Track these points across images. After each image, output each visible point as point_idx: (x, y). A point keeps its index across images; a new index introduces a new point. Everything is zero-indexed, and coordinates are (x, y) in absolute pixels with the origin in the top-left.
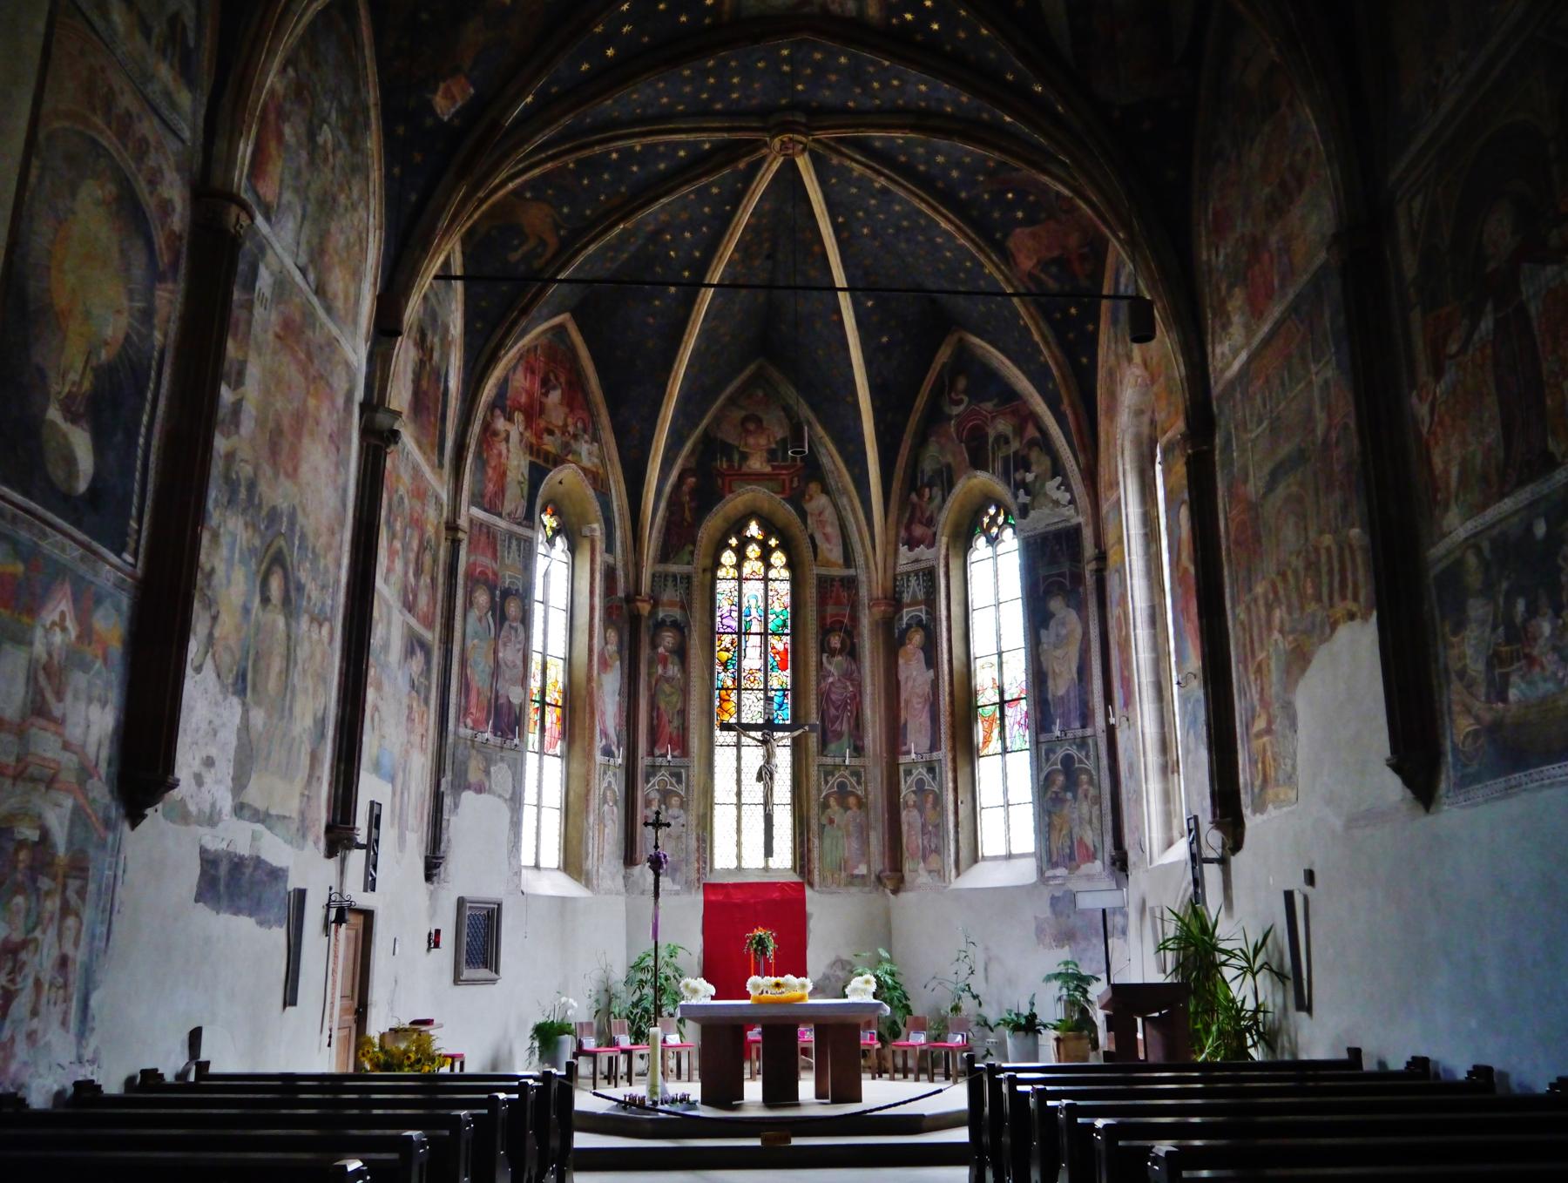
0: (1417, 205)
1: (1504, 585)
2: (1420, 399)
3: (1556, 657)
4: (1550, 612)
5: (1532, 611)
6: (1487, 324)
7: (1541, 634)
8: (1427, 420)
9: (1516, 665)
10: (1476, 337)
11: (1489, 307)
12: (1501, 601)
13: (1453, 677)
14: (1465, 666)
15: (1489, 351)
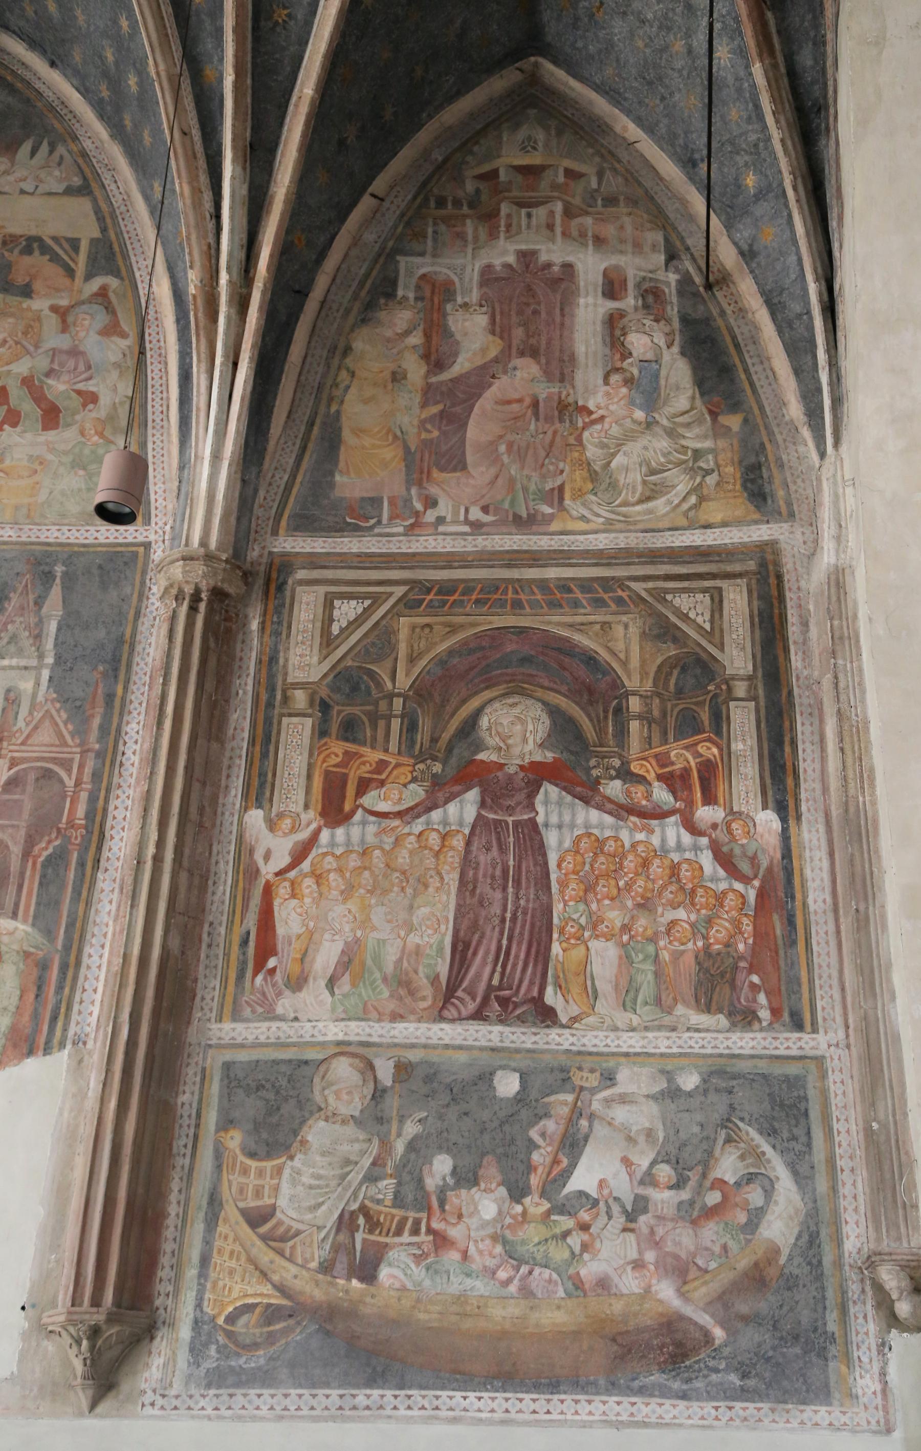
0: (346, 611)
1: (411, 1129)
2: (272, 825)
3: (499, 1249)
4: (503, 1191)
5: (466, 1178)
6: (465, 808)
7: (476, 1211)
8: (282, 860)
9: (406, 1238)
10: (436, 815)
11: (473, 795)
12: (400, 1147)
13: (231, 1212)
14: (274, 1208)
15: (458, 843)
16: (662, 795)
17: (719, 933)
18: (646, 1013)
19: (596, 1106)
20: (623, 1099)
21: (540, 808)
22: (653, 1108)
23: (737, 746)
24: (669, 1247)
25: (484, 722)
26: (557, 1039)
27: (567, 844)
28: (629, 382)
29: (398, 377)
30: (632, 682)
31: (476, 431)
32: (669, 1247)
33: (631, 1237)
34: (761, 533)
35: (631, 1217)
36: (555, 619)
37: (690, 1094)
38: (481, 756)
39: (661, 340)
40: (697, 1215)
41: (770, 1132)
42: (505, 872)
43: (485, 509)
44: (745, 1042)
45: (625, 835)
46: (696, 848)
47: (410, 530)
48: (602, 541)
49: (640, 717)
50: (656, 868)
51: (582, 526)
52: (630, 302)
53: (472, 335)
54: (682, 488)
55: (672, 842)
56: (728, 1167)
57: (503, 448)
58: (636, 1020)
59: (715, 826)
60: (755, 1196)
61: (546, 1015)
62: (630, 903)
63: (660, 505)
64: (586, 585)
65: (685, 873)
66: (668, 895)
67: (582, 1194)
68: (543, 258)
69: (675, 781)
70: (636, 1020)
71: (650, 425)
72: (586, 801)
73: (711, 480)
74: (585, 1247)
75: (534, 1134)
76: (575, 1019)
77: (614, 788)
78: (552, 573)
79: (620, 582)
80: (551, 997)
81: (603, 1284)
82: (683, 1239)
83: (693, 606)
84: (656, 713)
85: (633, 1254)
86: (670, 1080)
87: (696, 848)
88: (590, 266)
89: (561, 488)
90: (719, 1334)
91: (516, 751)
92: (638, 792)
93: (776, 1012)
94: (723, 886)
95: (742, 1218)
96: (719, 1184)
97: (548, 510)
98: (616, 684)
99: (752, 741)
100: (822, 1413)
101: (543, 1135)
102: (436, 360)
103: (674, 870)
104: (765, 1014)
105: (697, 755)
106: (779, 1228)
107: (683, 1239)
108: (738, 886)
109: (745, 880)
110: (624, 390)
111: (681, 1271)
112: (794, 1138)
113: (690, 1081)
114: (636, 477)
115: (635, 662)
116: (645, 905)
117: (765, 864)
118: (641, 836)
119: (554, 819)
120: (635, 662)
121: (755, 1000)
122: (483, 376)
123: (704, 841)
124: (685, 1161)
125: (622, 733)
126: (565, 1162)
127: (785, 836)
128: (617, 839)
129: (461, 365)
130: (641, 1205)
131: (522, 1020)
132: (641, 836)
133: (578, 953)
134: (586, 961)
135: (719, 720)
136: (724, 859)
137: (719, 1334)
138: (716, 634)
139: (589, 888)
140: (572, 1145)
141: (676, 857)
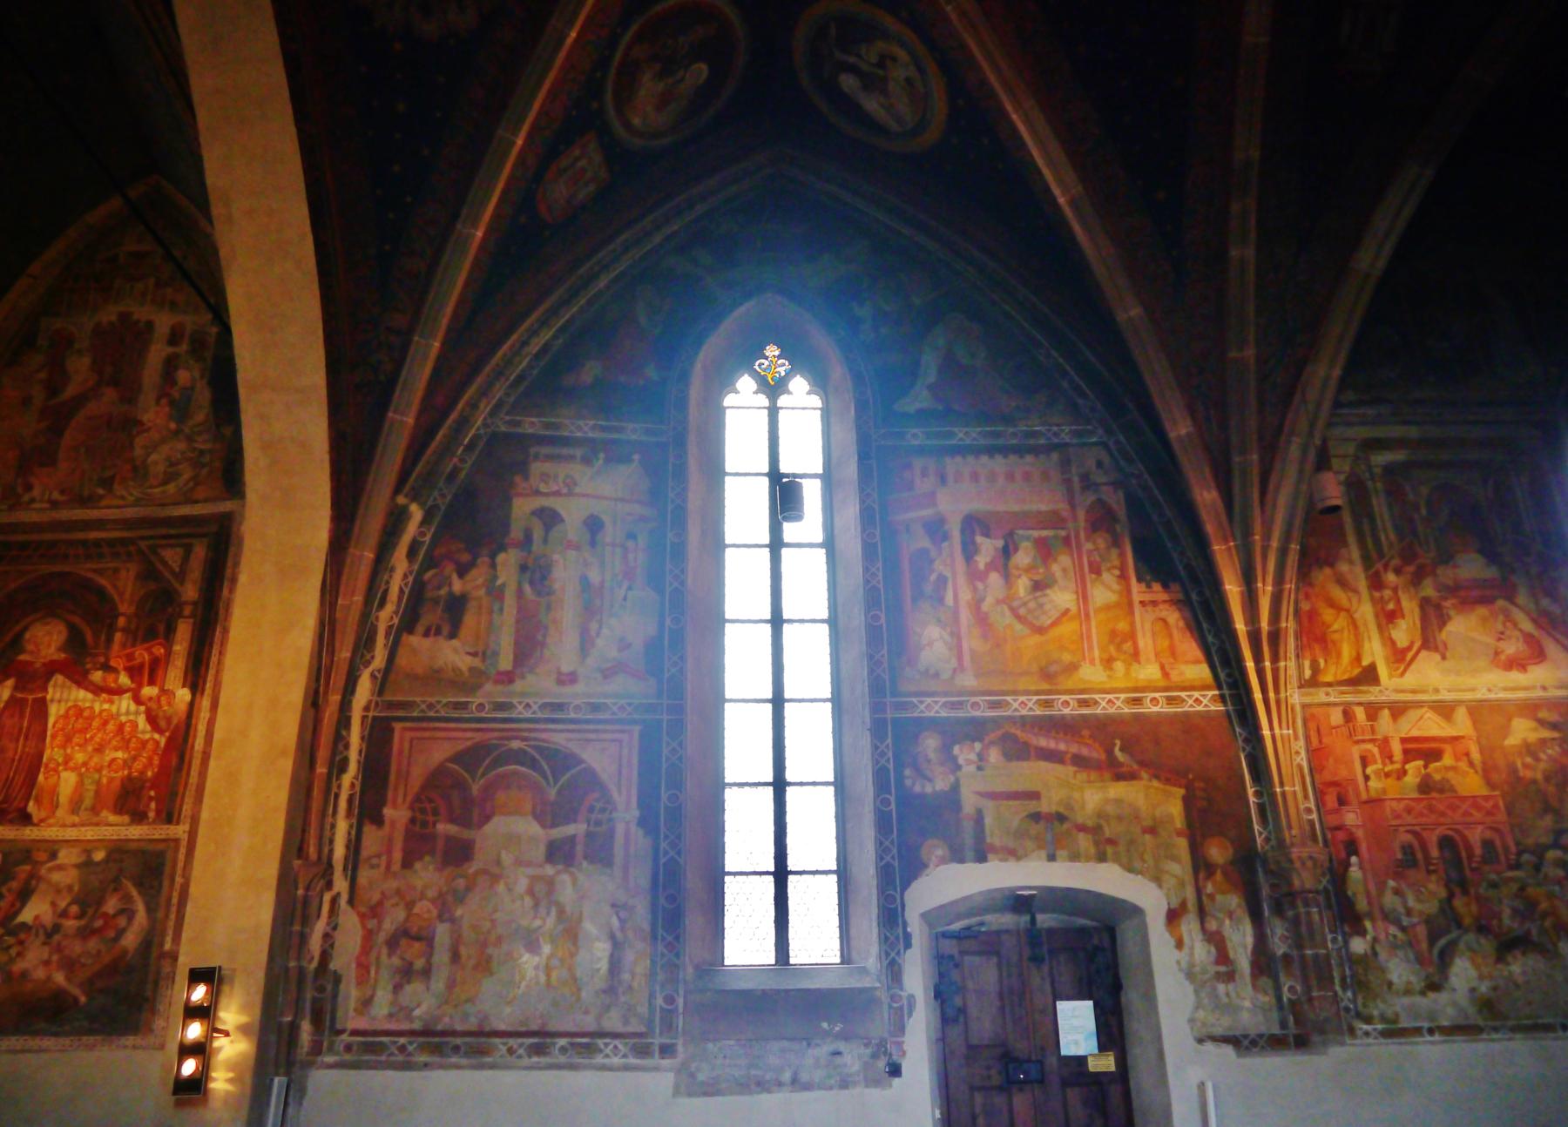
11: (10, 683)
16: (124, 680)
17: (138, 766)
18: (84, 815)
19: (43, 871)
20: (60, 868)
21: (50, 690)
22: (74, 873)
23: (177, 648)
24: (67, 952)
25: (27, 635)
26: (29, 833)
27: (62, 712)
28: (172, 403)
29: (26, 401)
30: (123, 608)
31: (68, 438)
32: (67, 952)
33: (46, 949)
34: (226, 506)
35: (49, 935)
36: (88, 566)
37: (98, 864)
38: (22, 657)
39: (197, 374)
40: (85, 933)
41: (139, 885)
42: (21, 729)
43: (62, 492)
44: (136, 832)
45: (97, 708)
46: (137, 713)
47: (11, 508)
48: (130, 513)
49: (123, 630)
50: (111, 727)
51: (121, 502)
52: (184, 347)
53: (80, 367)
54: (186, 477)
55: (123, 709)
56: (111, 905)
57: (83, 450)
58: (76, 819)
59: (151, 699)
60: (122, 921)
61: (26, 819)
62: (90, 748)
63: (171, 488)
64: (111, 543)
65: (127, 729)
66: (114, 743)
67: (24, 925)
68: (135, 317)
69: (134, 672)
70: (76, 819)
71: (176, 433)
72: (80, 685)
73: (205, 471)
74: (19, 954)
75: (4, 890)
76: (42, 821)
77: (97, 676)
78: (94, 535)
79: (132, 541)
80: (31, 807)
81: (24, 975)
82: (77, 948)
83: (172, 556)
84: (133, 626)
85: (46, 956)
86: (89, 856)
87: (137, 713)
88: (164, 322)
89: (112, 478)
90: (83, 999)
91: (43, 653)
92: (111, 677)
93: (158, 812)
94: (147, 736)
95: (112, 934)
96: (105, 915)
97: (101, 491)
98: (114, 608)
99: (186, 645)
100: (130, 1040)
101: (9, 890)
102: (53, 389)
103: (121, 727)
104: (152, 815)
105: (151, 653)
106: (130, 940)
107: (77, 948)
108: (157, 736)
109: (161, 732)
110: (167, 409)
111: (70, 965)
112: (152, 887)
113: (99, 856)
114: (161, 468)
115: (127, 596)
116: (99, 750)
117: (175, 721)
118: (106, 706)
119: (58, 696)
120: (127, 596)
121: (148, 805)
122: (80, 400)
123: (142, 708)
124: (88, 900)
125: (109, 641)
126: (18, 905)
127: (192, 705)
128: (91, 708)
129: (70, 391)
130: (57, 928)
131: (11, 822)
132: (106, 706)
133: (53, 780)
134: (56, 785)
135: (170, 631)
136: (152, 719)
137: (83, 999)
138: (181, 576)
139: (68, 740)
140: (24, 895)
141: (123, 719)
